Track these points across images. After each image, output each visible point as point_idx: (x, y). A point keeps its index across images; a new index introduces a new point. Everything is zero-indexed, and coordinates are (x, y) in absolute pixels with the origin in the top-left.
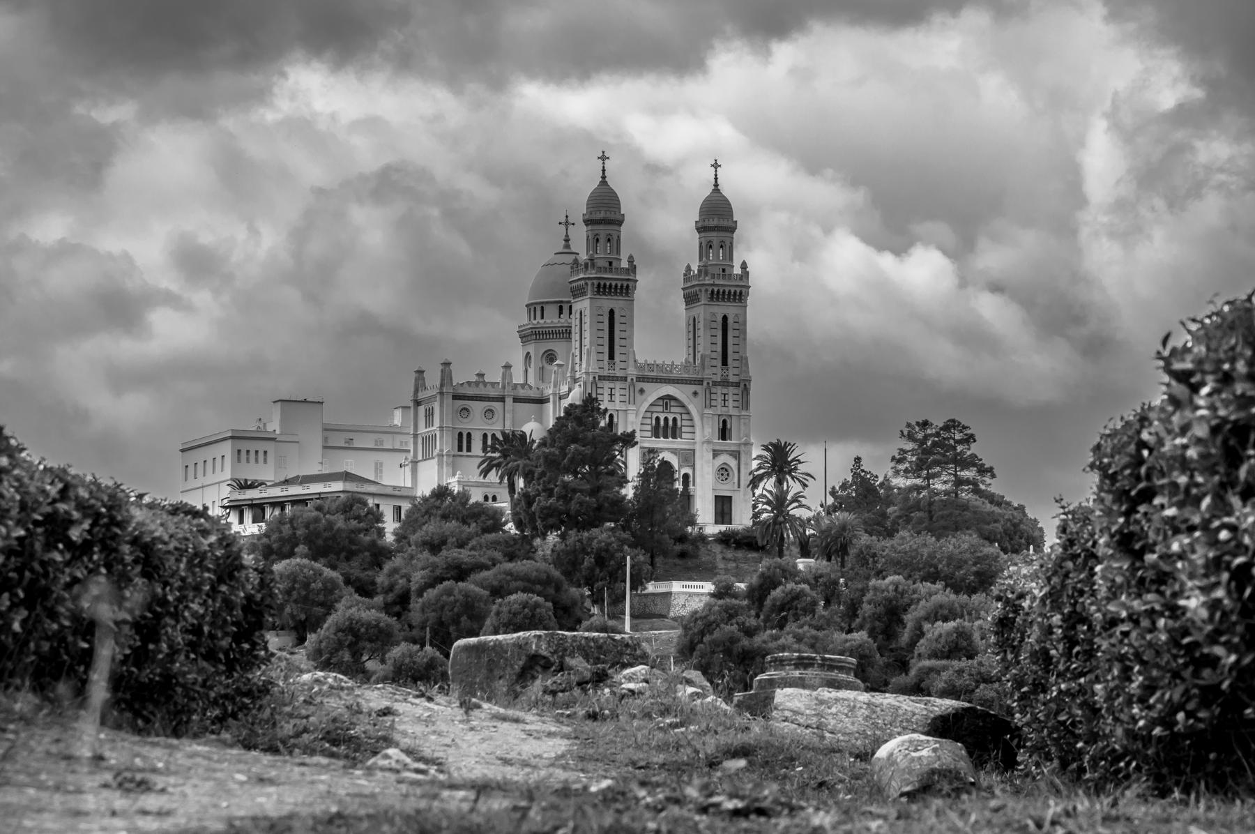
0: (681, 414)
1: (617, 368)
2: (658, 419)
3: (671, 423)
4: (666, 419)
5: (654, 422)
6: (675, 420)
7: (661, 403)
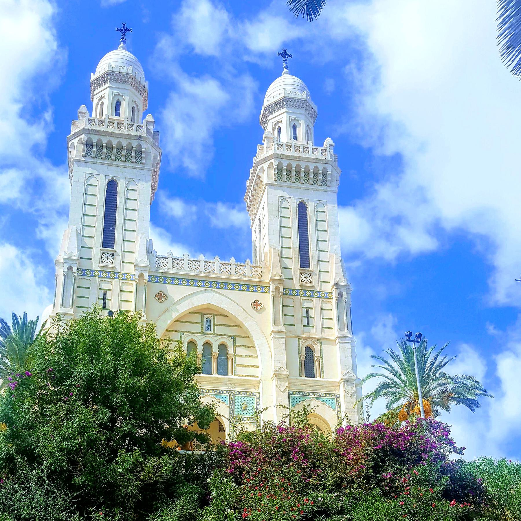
0: (234, 337)
2: (192, 344)
3: (215, 350)
4: (207, 345)
5: (185, 348)
6: (223, 347)
7: (198, 318)
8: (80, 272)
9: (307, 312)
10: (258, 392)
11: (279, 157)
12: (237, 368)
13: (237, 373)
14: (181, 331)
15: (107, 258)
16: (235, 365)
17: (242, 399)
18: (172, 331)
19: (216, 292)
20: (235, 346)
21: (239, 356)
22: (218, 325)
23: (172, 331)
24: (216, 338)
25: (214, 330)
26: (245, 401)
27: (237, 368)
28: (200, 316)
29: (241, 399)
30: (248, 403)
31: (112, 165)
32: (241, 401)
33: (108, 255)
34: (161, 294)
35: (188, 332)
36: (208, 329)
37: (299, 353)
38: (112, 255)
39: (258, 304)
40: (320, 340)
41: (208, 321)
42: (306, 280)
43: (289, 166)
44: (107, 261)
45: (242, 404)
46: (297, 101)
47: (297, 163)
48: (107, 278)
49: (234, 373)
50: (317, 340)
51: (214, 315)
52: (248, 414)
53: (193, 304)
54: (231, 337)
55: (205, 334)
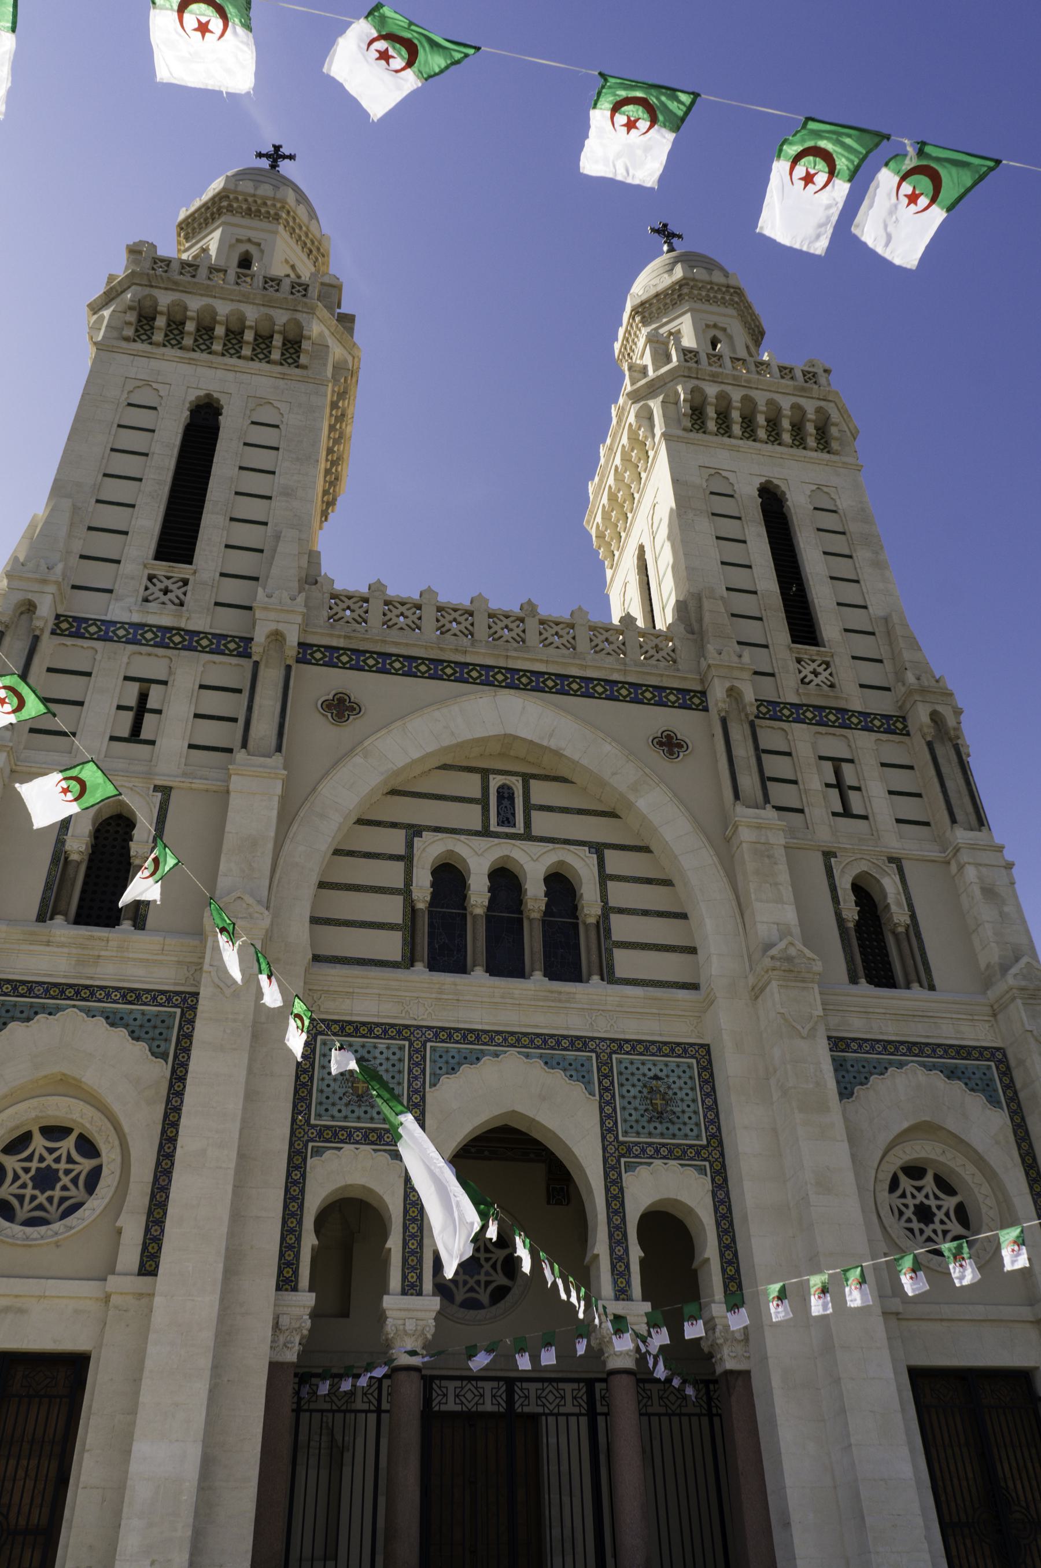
0: (598, 849)
1: (198, 598)
3: (535, 893)
7: (471, 786)
9: (838, 773)
10: (702, 1046)
13: (619, 973)
14: (408, 827)
15: (166, 591)
17: (646, 1071)
18: (378, 824)
20: (604, 878)
21: (621, 911)
23: (378, 824)
25: (528, 824)
26: (656, 1077)
28: (477, 778)
29: (641, 1072)
30: (669, 1087)
32: (642, 1078)
35: (437, 829)
36: (506, 819)
40: (896, 861)
41: (505, 795)
42: (817, 681)
43: (723, 397)
44: (165, 599)
45: (645, 1091)
46: (716, 288)
47: (743, 392)
48: (156, 645)
51: (526, 778)
52: (674, 1129)
53: (453, 734)
54: (587, 849)
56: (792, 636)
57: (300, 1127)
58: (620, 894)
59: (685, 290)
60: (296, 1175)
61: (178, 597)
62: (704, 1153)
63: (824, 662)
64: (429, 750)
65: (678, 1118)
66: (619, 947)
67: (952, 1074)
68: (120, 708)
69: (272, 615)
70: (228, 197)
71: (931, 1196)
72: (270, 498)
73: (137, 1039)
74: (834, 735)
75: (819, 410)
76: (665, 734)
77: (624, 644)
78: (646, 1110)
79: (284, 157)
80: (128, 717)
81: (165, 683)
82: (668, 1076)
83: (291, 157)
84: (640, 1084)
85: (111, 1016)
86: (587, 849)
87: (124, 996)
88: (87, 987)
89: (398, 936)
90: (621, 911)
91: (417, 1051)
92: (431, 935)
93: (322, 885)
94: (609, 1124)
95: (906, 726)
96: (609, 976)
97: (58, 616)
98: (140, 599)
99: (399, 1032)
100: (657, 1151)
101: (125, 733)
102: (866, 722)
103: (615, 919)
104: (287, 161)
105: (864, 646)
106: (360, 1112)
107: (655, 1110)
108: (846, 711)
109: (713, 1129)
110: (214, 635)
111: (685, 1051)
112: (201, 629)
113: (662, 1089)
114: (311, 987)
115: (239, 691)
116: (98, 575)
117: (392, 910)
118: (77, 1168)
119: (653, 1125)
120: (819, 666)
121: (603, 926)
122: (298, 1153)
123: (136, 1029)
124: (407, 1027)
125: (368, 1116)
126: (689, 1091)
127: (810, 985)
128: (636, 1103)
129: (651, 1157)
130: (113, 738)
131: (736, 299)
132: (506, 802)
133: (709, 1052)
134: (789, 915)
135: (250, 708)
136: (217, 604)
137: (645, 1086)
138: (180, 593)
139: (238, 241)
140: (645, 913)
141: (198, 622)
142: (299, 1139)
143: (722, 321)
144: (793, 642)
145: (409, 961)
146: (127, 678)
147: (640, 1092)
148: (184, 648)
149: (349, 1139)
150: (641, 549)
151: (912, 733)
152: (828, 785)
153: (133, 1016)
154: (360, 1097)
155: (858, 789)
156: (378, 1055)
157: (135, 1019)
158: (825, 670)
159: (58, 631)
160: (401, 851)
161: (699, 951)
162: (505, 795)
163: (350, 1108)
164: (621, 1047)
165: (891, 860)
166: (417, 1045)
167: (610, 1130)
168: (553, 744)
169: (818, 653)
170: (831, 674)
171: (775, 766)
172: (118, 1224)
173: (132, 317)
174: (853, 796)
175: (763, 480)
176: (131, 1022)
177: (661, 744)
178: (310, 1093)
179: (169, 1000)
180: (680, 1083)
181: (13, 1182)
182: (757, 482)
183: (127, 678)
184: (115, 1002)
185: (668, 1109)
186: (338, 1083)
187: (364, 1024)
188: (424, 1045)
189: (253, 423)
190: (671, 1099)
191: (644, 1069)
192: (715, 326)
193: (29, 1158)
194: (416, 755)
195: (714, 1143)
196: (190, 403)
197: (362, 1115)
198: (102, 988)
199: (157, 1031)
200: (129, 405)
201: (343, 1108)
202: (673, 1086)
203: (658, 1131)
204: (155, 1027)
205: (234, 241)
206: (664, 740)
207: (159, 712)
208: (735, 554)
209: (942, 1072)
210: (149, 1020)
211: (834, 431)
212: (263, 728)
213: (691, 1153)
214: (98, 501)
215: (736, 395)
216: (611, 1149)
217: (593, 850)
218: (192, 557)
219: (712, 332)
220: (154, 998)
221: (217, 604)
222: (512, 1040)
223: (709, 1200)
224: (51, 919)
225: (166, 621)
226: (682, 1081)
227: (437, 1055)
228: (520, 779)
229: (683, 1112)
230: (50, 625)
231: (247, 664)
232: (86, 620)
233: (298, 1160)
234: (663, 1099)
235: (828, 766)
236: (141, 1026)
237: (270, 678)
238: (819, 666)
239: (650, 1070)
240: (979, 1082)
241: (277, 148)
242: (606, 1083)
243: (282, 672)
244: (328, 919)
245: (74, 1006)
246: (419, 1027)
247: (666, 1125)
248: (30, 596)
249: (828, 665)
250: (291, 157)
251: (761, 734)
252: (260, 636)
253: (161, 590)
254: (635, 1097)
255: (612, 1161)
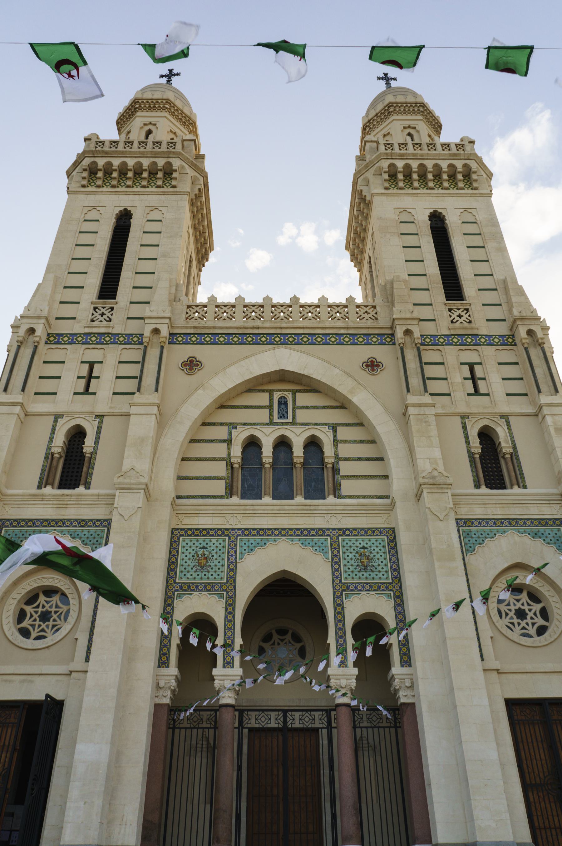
0: (334, 427)
5: (237, 451)
7: (263, 399)
8: (52, 339)
10: (390, 529)
11: (390, 157)
12: (343, 482)
13: (344, 493)
15: (102, 315)
16: (337, 478)
17: (358, 545)
19: (291, 349)
20: (336, 442)
21: (345, 459)
22: (303, 408)
24: (298, 430)
25: (294, 417)
26: (364, 548)
27: (343, 482)
29: (355, 545)
30: (371, 553)
31: (126, 193)
32: (356, 548)
33: (103, 310)
34: (192, 361)
35: (245, 424)
36: (283, 415)
37: (467, 442)
38: (110, 310)
39: (375, 363)
40: (505, 417)
41: (283, 403)
42: (460, 320)
43: (407, 167)
45: (357, 555)
48: (97, 344)
49: (337, 493)
50: (499, 417)
51: (294, 392)
52: (373, 575)
53: (251, 373)
54: (327, 427)
55: (277, 424)
56: (446, 297)
57: (171, 584)
58: (345, 450)
59: (392, 110)
60: (169, 609)
61: (108, 317)
62: (390, 587)
63: (465, 309)
64: (238, 383)
65: (376, 568)
66: (344, 479)
67: (535, 535)
68: (79, 377)
69: (153, 321)
70: (138, 102)
71: (525, 604)
72: (156, 259)
73: (86, 544)
74: (470, 350)
75: (465, 166)
76: (370, 360)
77: (348, 313)
78: (358, 565)
79: (175, 75)
80: (83, 382)
81: (101, 362)
82: (370, 547)
83: (178, 74)
84: (355, 551)
85: (73, 534)
86: (327, 427)
87: (79, 523)
88: (61, 520)
89: (222, 483)
90: (345, 459)
91: (232, 542)
92: (243, 480)
93: (184, 459)
94: (337, 574)
95: (514, 340)
96: (337, 493)
97: (48, 334)
98: (89, 320)
99: (223, 532)
100: (364, 587)
101: (81, 390)
102: (490, 340)
103: (341, 463)
104: (176, 76)
105: (491, 297)
106: (202, 575)
107: (363, 565)
108: (477, 335)
109: (396, 574)
110: (126, 335)
111: (380, 532)
112: (120, 332)
113: (367, 554)
114: (178, 512)
115: (139, 362)
116: (69, 310)
117: (221, 469)
118: (61, 610)
119: (361, 573)
120: (462, 312)
121: (335, 468)
122: (170, 597)
123: (85, 540)
124: (227, 529)
125: (206, 577)
126: (382, 554)
127: (446, 491)
128: (352, 562)
129: (360, 590)
130: (75, 394)
131: (421, 109)
132: (283, 406)
133: (394, 532)
134: (437, 453)
135: (142, 371)
136: (128, 318)
137: (357, 553)
138: (109, 315)
139: (145, 125)
140: (359, 459)
141: (117, 330)
142: (170, 590)
143: (412, 123)
144: (447, 300)
145: (230, 494)
146: (82, 362)
147: (354, 556)
148: (111, 343)
149: (196, 589)
150: (370, 257)
151: (517, 344)
152: (465, 379)
153: (83, 533)
154: (202, 567)
155: (484, 379)
156: (212, 545)
157: (85, 535)
158: (466, 314)
159: (49, 342)
160: (225, 437)
161: (389, 478)
162: (283, 403)
163: (197, 573)
164: (344, 532)
165: (502, 416)
166: (233, 538)
167: (337, 577)
168: (305, 372)
169: (462, 304)
170: (469, 316)
171: (430, 371)
172: (75, 637)
173: (85, 174)
174: (481, 384)
175: (432, 210)
176: (83, 536)
177: (367, 366)
178: (176, 567)
179: (101, 524)
180: (377, 550)
181: (30, 618)
182: (428, 212)
183: (82, 362)
184: (75, 526)
185: (370, 564)
186: (191, 561)
187: (204, 529)
188: (236, 538)
189: (148, 221)
190: (372, 559)
191: (357, 544)
192: (409, 127)
193: (38, 607)
194: (231, 385)
195: (396, 581)
196: (117, 214)
197: (203, 576)
198: (68, 520)
199: (96, 540)
200: (85, 220)
201: (193, 574)
202: (373, 552)
203: (364, 576)
204: (94, 538)
205: (142, 125)
206: (369, 363)
207: (98, 378)
208: (413, 254)
209: (529, 534)
210: (91, 535)
211: (474, 177)
212: (149, 380)
213: (382, 587)
214: (69, 273)
215: (415, 165)
216: (337, 587)
217: (331, 428)
218: (116, 295)
219: (407, 131)
220: (94, 523)
221: (128, 318)
222: (283, 532)
223: (392, 612)
224: (45, 487)
225: (102, 330)
226: (378, 549)
227: (243, 543)
228: (290, 393)
229: (379, 565)
230: (44, 338)
231: (142, 347)
232: (62, 335)
233: (169, 601)
234: (368, 559)
235: (467, 368)
236: (88, 538)
237: (153, 354)
238: (462, 312)
239: (360, 544)
240: (552, 539)
241: (171, 71)
242: (335, 552)
243: (159, 350)
244: (187, 476)
245: (55, 530)
246: (233, 529)
247: (368, 573)
248: (32, 326)
249: (467, 310)
250: (178, 74)
251: (423, 353)
252: (147, 333)
253: (100, 314)
254: (351, 559)
255: (338, 594)
